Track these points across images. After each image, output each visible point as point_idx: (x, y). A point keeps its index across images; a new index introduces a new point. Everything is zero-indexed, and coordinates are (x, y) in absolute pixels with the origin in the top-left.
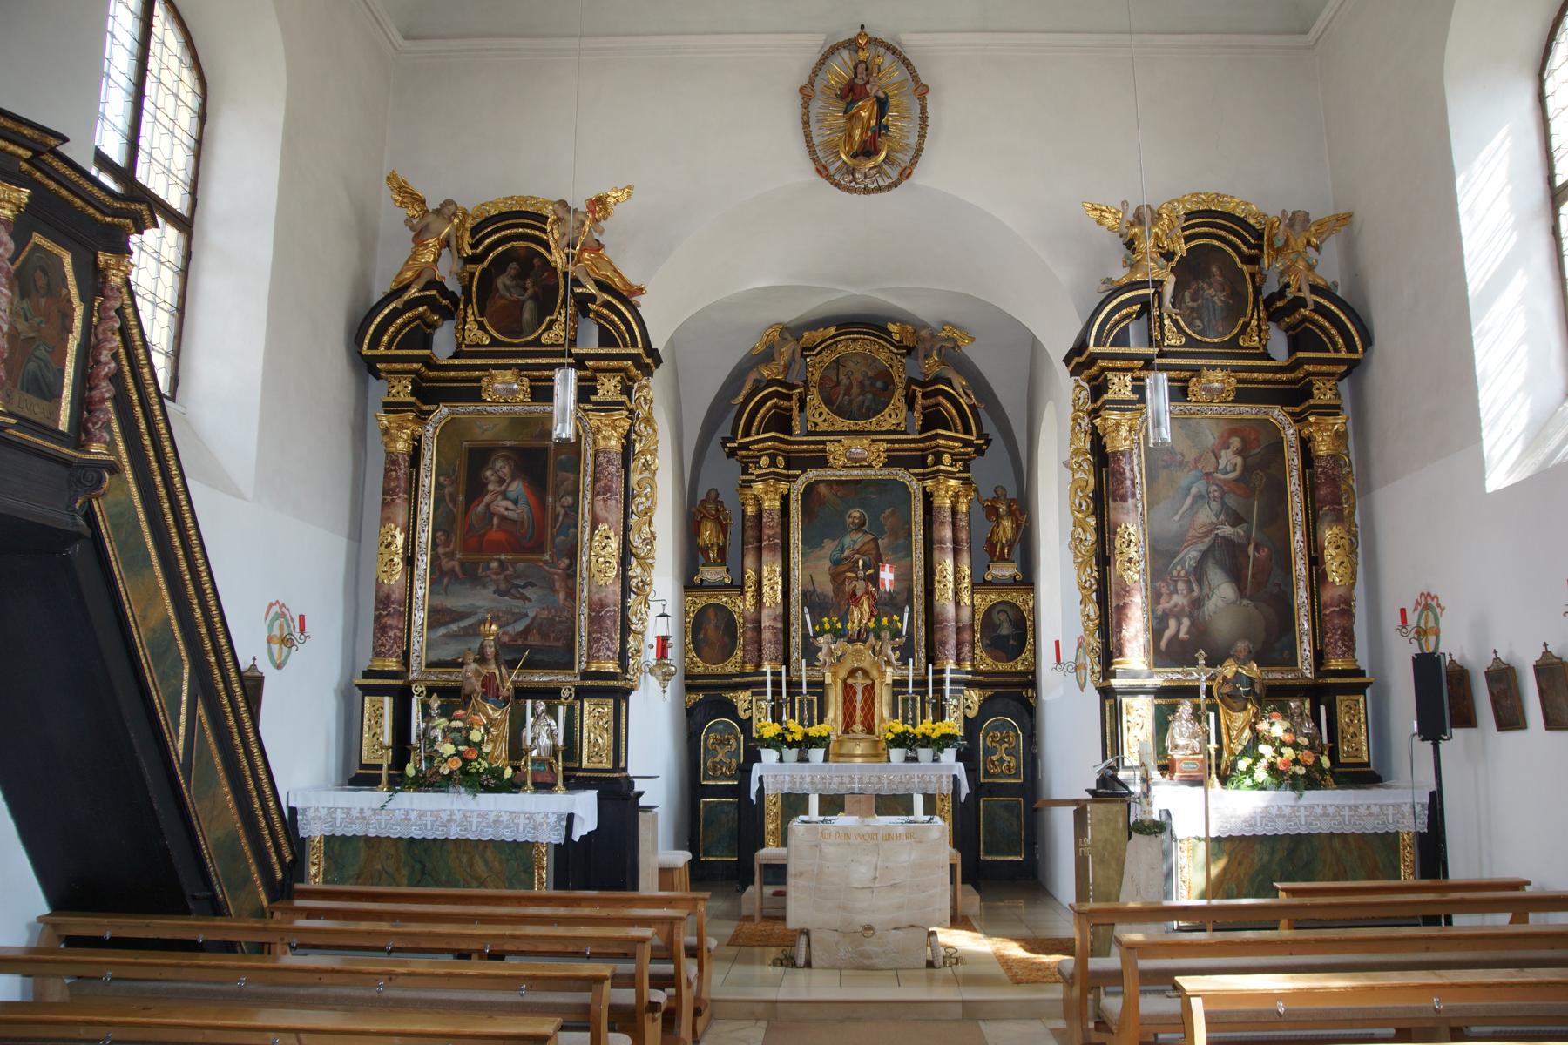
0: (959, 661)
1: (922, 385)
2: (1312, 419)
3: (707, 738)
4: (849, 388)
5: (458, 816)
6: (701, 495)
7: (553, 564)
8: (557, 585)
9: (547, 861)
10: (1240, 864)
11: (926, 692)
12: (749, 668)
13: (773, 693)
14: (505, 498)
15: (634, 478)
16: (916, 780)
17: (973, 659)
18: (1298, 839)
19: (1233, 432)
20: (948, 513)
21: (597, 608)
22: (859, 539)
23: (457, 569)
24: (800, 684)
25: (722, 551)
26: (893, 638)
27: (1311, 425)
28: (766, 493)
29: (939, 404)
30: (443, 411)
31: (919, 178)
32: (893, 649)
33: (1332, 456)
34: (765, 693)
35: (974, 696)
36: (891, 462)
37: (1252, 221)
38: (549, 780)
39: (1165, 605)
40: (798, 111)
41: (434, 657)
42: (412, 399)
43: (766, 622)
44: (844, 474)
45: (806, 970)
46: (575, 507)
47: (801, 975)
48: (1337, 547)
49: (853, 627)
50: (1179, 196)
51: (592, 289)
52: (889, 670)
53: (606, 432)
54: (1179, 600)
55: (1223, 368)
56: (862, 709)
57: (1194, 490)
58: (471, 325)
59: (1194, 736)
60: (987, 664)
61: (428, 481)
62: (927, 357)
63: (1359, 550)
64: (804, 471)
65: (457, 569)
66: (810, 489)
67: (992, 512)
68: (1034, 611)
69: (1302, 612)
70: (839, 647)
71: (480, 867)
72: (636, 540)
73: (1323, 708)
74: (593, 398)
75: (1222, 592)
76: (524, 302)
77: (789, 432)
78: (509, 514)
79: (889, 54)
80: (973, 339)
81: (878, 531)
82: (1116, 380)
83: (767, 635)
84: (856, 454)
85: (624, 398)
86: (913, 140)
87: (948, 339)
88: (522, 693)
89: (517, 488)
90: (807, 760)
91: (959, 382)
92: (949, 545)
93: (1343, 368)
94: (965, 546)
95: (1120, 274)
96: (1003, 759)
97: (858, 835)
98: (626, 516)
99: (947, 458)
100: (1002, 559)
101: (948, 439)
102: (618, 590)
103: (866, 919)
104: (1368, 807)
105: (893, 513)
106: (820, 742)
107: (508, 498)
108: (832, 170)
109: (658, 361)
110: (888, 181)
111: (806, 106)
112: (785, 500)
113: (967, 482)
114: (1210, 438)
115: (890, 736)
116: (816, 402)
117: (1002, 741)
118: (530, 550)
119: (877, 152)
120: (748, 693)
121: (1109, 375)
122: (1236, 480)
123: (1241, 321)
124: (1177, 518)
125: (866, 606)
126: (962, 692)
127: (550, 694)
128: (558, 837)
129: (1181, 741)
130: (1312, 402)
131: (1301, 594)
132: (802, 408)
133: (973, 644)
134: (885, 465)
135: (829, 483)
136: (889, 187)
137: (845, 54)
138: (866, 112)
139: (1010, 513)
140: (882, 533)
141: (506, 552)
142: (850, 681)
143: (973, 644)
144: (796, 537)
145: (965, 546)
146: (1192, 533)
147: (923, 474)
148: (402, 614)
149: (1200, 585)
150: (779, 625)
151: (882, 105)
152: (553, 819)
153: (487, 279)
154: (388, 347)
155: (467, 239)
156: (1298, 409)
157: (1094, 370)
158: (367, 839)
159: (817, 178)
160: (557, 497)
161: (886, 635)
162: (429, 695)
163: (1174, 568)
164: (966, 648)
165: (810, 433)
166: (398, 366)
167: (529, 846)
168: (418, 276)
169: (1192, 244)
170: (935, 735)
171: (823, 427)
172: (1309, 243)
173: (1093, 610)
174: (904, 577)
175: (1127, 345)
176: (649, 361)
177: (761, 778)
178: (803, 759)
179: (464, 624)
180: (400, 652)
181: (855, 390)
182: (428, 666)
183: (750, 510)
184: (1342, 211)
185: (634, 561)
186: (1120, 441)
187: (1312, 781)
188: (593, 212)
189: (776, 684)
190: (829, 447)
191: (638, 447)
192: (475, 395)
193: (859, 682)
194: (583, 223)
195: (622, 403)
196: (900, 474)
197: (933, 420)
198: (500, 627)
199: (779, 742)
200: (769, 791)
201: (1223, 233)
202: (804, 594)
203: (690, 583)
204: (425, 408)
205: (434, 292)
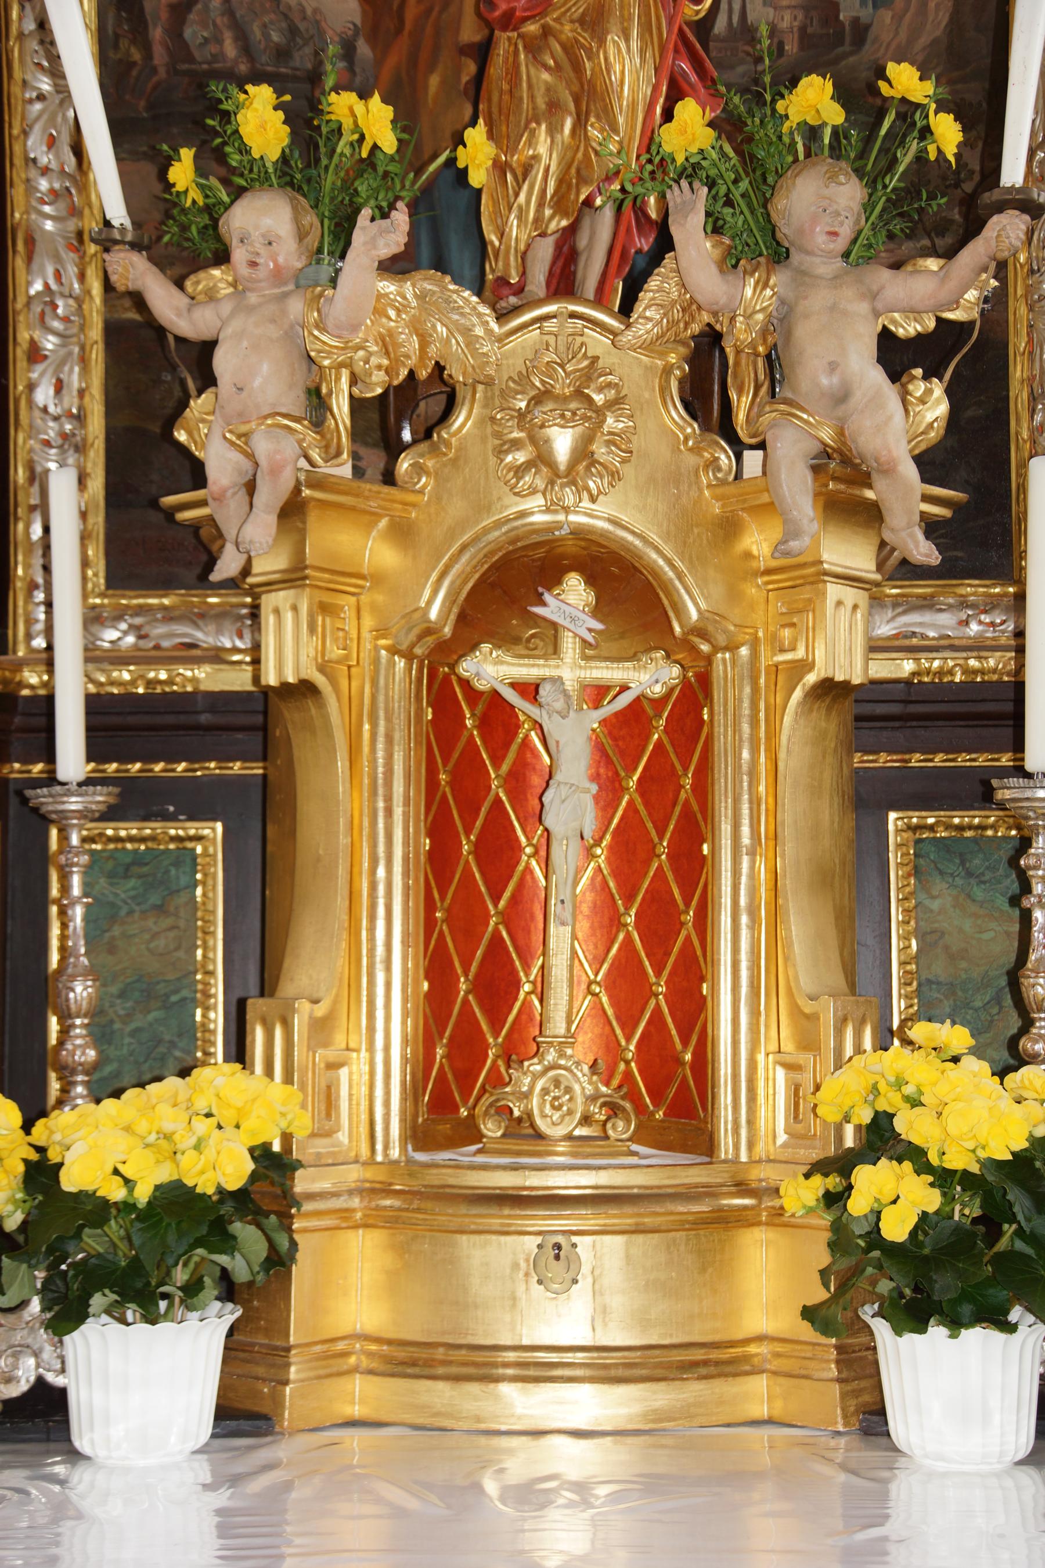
32: (896, 356)
52: (850, 553)
70: (381, 312)
142: (490, 668)
161: (823, 204)
193: (568, 675)
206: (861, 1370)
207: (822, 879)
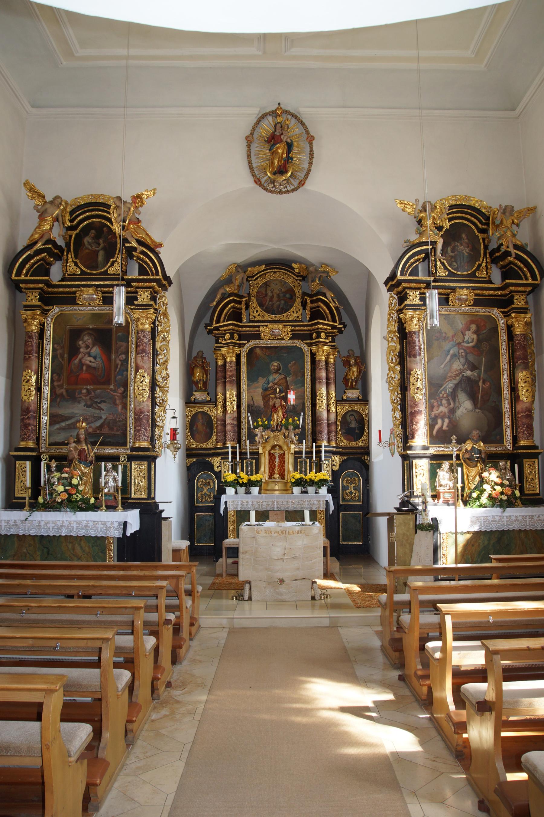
0: (329, 441)
1: (310, 296)
2: (513, 315)
3: (199, 482)
4: (272, 297)
5: (66, 524)
6: (194, 354)
7: (115, 391)
8: (118, 402)
9: (113, 547)
10: (473, 545)
11: (312, 457)
12: (219, 445)
13: (232, 458)
14: (90, 356)
15: (158, 345)
16: (307, 503)
17: (336, 440)
18: (503, 533)
19: (472, 322)
20: (324, 363)
21: (138, 414)
22: (277, 377)
23: (64, 393)
24: (246, 453)
25: (205, 384)
26: (295, 429)
27: (512, 318)
28: (228, 353)
29: (319, 306)
30: (56, 310)
31: (309, 185)
32: (295, 435)
33: (523, 335)
34: (228, 458)
35: (337, 459)
36: (294, 336)
37: (484, 211)
38: (114, 504)
39: (435, 412)
40: (245, 149)
41: (53, 440)
42: (39, 303)
43: (228, 421)
44: (269, 343)
45: (249, 602)
46: (126, 360)
47: (246, 605)
48: (525, 382)
49: (273, 423)
50: (446, 197)
51: (134, 244)
52: (293, 446)
53: (143, 320)
54: (443, 409)
55: (467, 288)
56: (279, 466)
57: (451, 352)
58: (70, 264)
59: (450, 480)
60: (344, 442)
61: (49, 347)
62: (313, 281)
63: (536, 384)
64: (248, 342)
65: (64, 393)
66: (251, 351)
67: (347, 363)
68: (368, 415)
69: (507, 416)
70: (267, 433)
71: (78, 550)
72: (159, 378)
73: (516, 466)
74: (136, 302)
75: (465, 405)
76: (98, 251)
77: (241, 321)
78: (92, 364)
79: (293, 119)
80: (337, 272)
81: (287, 373)
82: (411, 294)
83: (229, 428)
84: (276, 332)
85: (152, 302)
86: (306, 166)
87: (324, 272)
88: (100, 459)
89: (96, 350)
90: (250, 493)
91: (330, 294)
92: (324, 381)
93: (529, 289)
94: (333, 381)
95: (414, 238)
96: (351, 491)
97: (276, 532)
98: (154, 365)
99: (323, 335)
100: (352, 388)
101: (324, 325)
102: (150, 404)
103: (280, 575)
104: (539, 516)
105: (295, 363)
106: (257, 483)
107: (90, 356)
108: (263, 181)
109: (170, 283)
110: (292, 187)
111: (249, 147)
112: (238, 357)
113: (333, 347)
114: (460, 324)
115: (293, 480)
116: (254, 305)
117: (351, 483)
118: (103, 384)
119: (287, 172)
120: (219, 458)
121: (408, 291)
122: (473, 347)
123: (477, 263)
124: (442, 366)
125: (280, 413)
126: (330, 457)
127: (114, 459)
128: (118, 534)
129: (443, 482)
130: (513, 306)
131: (506, 406)
132: (247, 308)
133: (336, 432)
134: (290, 339)
135: (262, 348)
136: (293, 190)
137: (270, 118)
138: (281, 150)
139: (356, 363)
140: (289, 374)
141: (90, 384)
142: (272, 452)
143: (336, 432)
144: (244, 376)
145: (333, 381)
146: (450, 374)
147: (311, 343)
148: (35, 418)
149: (454, 402)
150: (235, 423)
151: (290, 146)
152: (116, 525)
153: (79, 238)
154: (26, 275)
155: (68, 217)
156: (506, 310)
157: (400, 289)
158: (18, 536)
159: (255, 185)
160: (117, 356)
161: (291, 427)
162: (50, 461)
163: (441, 392)
164: (333, 434)
165: (251, 321)
166: (31, 286)
167: (104, 539)
168: (41, 237)
169: (452, 222)
170: (317, 480)
171: (258, 318)
172: (513, 222)
173: (398, 414)
174: (300, 397)
175: (417, 275)
176: (165, 283)
177: (226, 502)
178: (248, 492)
179: (68, 422)
180: (34, 437)
181: (275, 299)
182: (49, 445)
183: (220, 362)
184: (531, 206)
185: (158, 389)
186: (414, 326)
187: (510, 503)
188: (135, 203)
189: (234, 453)
190: (261, 329)
191: (159, 328)
192: (73, 301)
193: (277, 452)
194: (130, 209)
195: (151, 305)
196: (298, 343)
197: (316, 315)
198: (87, 424)
199: (235, 484)
200: (230, 509)
201: (469, 217)
202: (248, 406)
203: (188, 401)
204: (46, 308)
205: (50, 246)
206: (292, 489)
207: (292, 464)
